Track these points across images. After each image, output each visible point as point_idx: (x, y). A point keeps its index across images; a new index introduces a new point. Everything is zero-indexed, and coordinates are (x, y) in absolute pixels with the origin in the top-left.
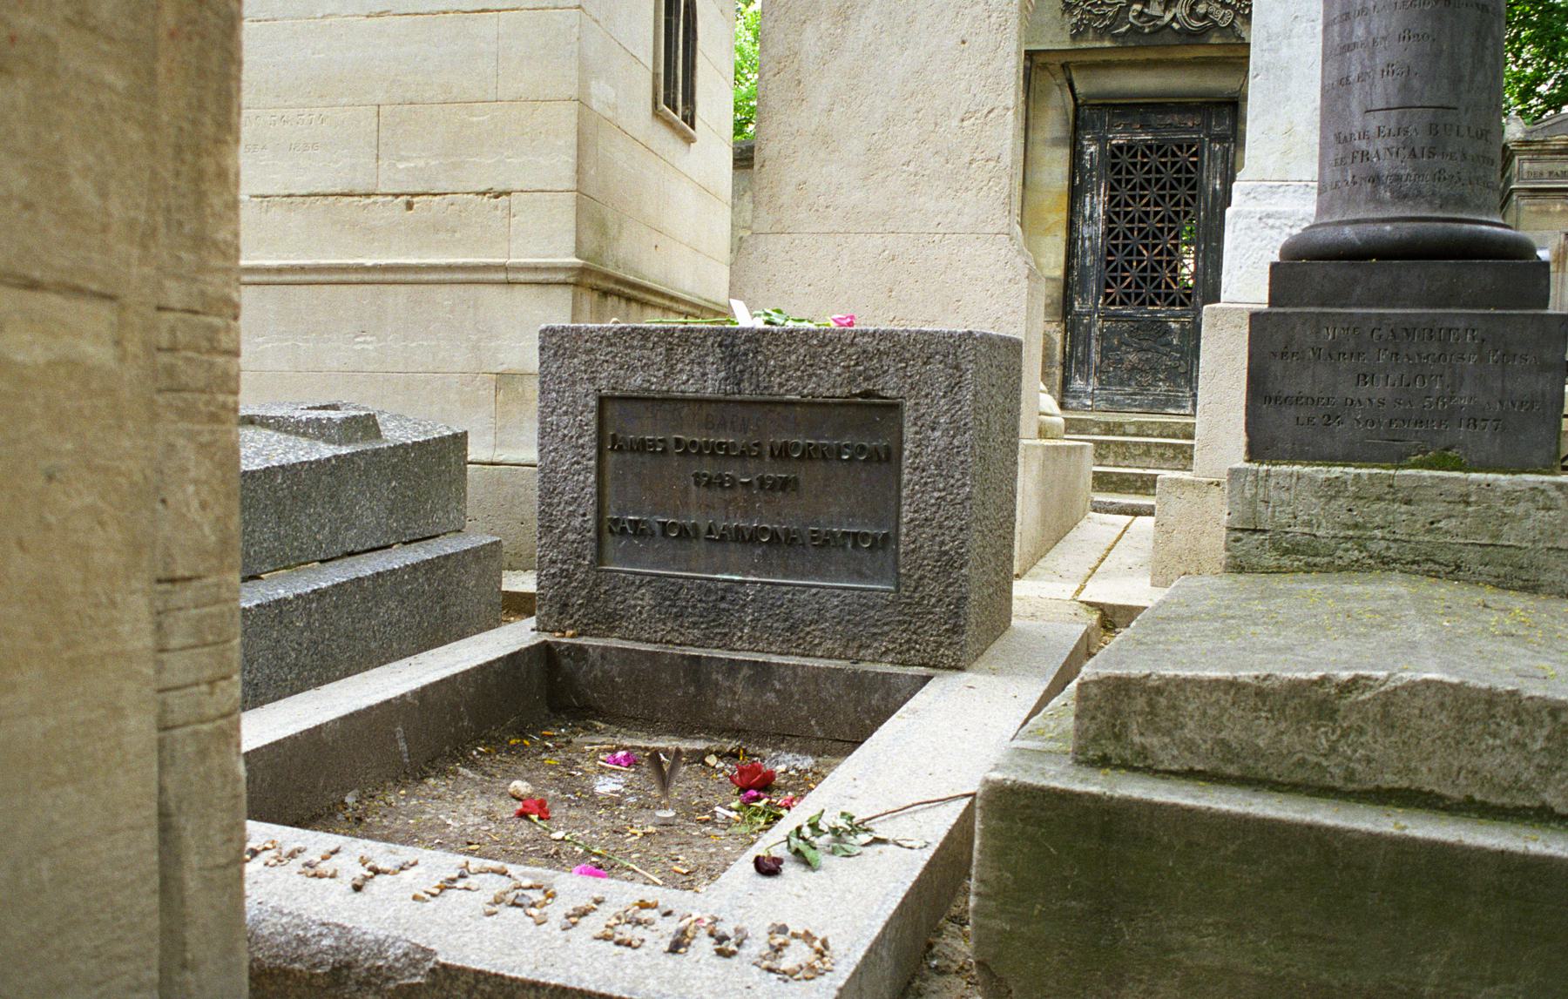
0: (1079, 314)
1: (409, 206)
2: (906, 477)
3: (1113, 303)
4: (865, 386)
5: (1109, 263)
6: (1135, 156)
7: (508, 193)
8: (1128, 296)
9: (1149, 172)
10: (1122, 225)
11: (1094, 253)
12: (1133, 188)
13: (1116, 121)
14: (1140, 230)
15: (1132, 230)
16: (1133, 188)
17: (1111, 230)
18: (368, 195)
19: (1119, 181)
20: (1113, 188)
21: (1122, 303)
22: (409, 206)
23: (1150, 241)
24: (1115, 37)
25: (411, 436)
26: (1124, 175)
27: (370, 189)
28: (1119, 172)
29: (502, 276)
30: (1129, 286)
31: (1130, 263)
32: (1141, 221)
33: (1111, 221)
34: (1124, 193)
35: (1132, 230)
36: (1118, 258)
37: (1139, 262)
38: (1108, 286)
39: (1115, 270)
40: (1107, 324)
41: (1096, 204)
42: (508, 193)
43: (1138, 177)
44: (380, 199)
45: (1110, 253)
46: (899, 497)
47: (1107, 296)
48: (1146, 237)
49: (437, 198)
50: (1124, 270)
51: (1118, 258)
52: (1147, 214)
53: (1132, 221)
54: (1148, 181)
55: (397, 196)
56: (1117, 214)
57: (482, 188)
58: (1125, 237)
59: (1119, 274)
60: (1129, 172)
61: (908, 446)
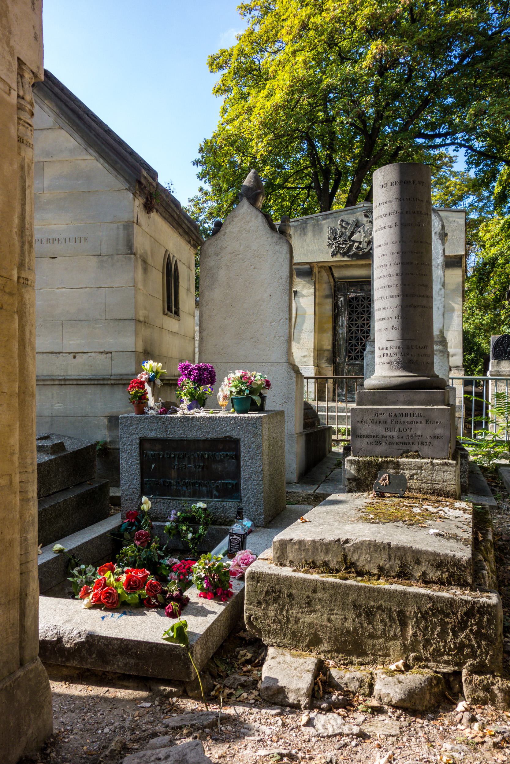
0: (339, 364)
1: (75, 357)
2: (242, 464)
3: (352, 359)
4: (228, 434)
5: (350, 343)
6: (358, 301)
7: (111, 353)
8: (358, 356)
9: (364, 307)
10: (354, 329)
11: (344, 339)
12: (358, 314)
13: (351, 288)
14: (361, 330)
15: (358, 330)
16: (358, 314)
17: (350, 331)
18: (59, 353)
19: (352, 312)
20: (350, 314)
21: (355, 359)
22: (75, 357)
23: (365, 335)
24: (349, 256)
25: (76, 447)
26: (354, 309)
27: (60, 351)
28: (353, 308)
29: (109, 382)
30: (358, 352)
31: (358, 343)
32: (362, 327)
33: (349, 327)
34: (355, 316)
35: (358, 330)
36: (354, 342)
37: (361, 343)
38: (350, 352)
39: (352, 346)
40: (350, 367)
41: (344, 321)
42: (111, 353)
43: (360, 310)
44: (64, 355)
45: (350, 340)
46: (240, 471)
47: (349, 356)
48: (364, 333)
49: (85, 355)
50: (356, 346)
51: (354, 342)
52: (364, 324)
53: (358, 327)
54: (364, 311)
55: (69, 353)
56: (352, 324)
57: (101, 351)
58: (356, 333)
59: (354, 348)
60: (356, 308)
61: (242, 454)
